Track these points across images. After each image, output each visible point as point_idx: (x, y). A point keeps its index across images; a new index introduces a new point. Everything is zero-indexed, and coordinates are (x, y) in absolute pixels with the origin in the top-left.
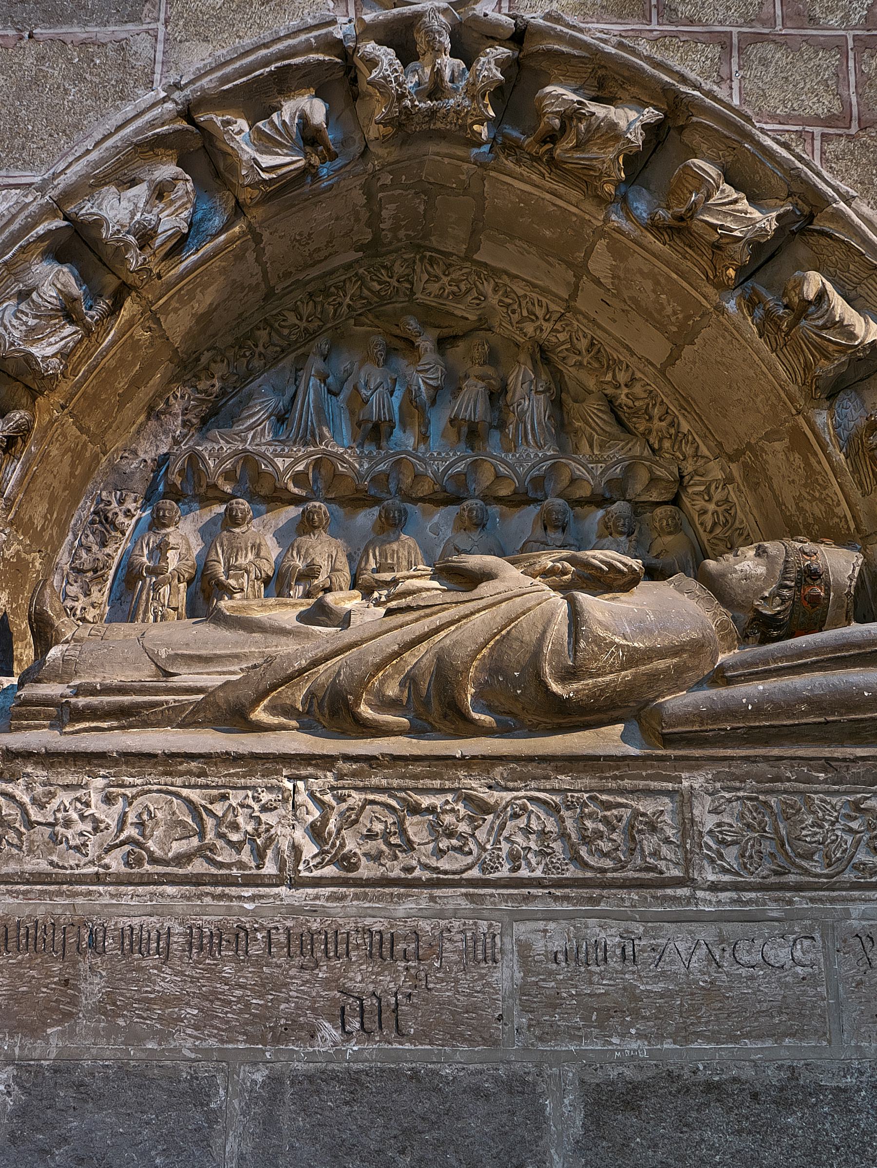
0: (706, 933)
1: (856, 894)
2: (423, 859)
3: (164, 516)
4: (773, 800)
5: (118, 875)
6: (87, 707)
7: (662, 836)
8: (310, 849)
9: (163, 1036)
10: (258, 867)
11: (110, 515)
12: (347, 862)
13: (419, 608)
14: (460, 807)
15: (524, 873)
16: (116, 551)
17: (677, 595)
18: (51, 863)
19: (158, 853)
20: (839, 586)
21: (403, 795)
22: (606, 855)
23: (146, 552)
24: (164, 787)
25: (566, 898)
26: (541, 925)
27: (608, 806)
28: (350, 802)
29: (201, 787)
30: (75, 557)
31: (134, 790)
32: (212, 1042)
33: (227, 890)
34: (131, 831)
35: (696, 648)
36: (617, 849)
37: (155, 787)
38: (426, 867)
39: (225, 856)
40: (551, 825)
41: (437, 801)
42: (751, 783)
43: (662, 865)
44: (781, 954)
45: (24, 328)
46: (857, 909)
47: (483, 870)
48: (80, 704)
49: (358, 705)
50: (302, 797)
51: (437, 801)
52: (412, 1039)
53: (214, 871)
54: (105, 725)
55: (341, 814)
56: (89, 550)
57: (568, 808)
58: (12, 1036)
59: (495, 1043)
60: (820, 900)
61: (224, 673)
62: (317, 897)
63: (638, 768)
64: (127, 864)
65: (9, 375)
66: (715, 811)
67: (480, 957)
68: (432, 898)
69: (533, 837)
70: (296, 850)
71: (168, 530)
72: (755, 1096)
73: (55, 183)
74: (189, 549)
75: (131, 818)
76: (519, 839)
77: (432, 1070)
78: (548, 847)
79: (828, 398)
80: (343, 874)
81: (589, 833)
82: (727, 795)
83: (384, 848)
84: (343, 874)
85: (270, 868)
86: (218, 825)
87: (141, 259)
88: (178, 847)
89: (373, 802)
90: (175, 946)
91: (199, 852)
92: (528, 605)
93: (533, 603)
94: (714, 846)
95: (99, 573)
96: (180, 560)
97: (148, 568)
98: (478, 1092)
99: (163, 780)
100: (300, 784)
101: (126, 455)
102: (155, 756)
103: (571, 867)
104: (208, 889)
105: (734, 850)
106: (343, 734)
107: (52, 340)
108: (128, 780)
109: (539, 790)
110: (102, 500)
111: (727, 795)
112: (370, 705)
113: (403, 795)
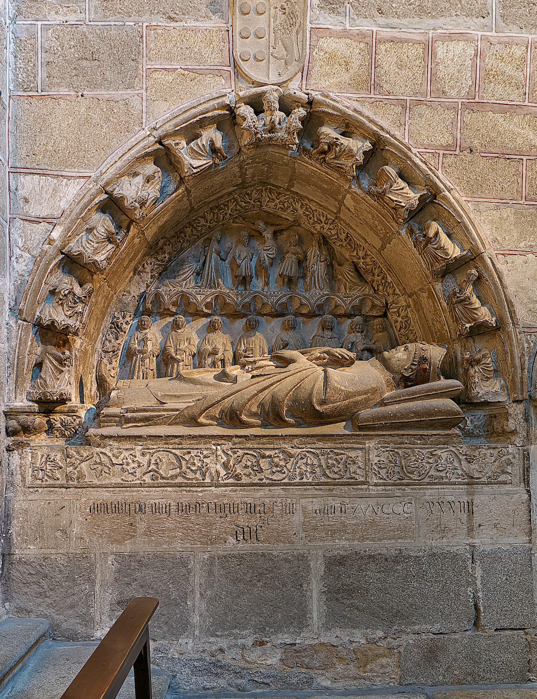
0: (372, 502)
1: (429, 486)
2: (266, 476)
3: (145, 324)
4: (400, 451)
5: (149, 484)
6: (132, 417)
7: (358, 466)
8: (223, 472)
9: (169, 543)
10: (203, 480)
11: (119, 324)
12: (237, 477)
13: (265, 375)
14: (281, 455)
15: (305, 480)
16: (122, 341)
17: (370, 368)
18: (122, 480)
19: (164, 475)
20: (435, 364)
21: (259, 451)
22: (336, 473)
23: (137, 342)
24: (165, 449)
25: (321, 489)
26: (311, 500)
27: (337, 454)
28: (238, 454)
29: (180, 449)
30: (104, 344)
31: (153, 451)
32: (188, 545)
33: (191, 489)
34: (153, 467)
35: (374, 391)
36: (340, 471)
37: (162, 449)
38: (268, 478)
39: (190, 475)
40: (315, 462)
41: (272, 453)
42: (392, 445)
43: (357, 476)
45: (92, 248)
46: (428, 492)
47: (289, 480)
48: (129, 416)
49: (241, 416)
50: (220, 452)
51: (272, 453)
52: (262, 542)
53: (186, 481)
54: (139, 425)
55: (234, 459)
56: (110, 342)
57: (322, 455)
58: (112, 544)
59: (293, 543)
61: (186, 402)
62: (226, 491)
63: (349, 439)
64: (152, 479)
65: (81, 265)
66: (378, 456)
67: (288, 512)
68: (270, 490)
69: (309, 466)
70: (217, 472)
71: (147, 331)
72: (386, 559)
73: (102, 177)
74: (157, 340)
75: (153, 461)
76: (303, 467)
77: (270, 553)
78: (314, 470)
79: (442, 277)
80: (236, 482)
81: (329, 465)
82: (383, 450)
83: (252, 472)
84: (236, 482)
85: (208, 480)
86: (187, 464)
87: (141, 213)
88: (171, 473)
89: (247, 454)
90: (172, 510)
91: (180, 474)
92: (308, 374)
93: (310, 373)
94: (377, 469)
95: (116, 353)
96: (153, 346)
97: (138, 350)
98: (286, 560)
99: (164, 446)
100: (219, 447)
101: (125, 293)
102: (162, 437)
103: (323, 478)
104: (184, 488)
105: (385, 470)
106: (235, 427)
107: (103, 252)
108: (151, 447)
109: (311, 448)
110: (115, 317)
111: (383, 450)
112: (246, 415)
113: (259, 451)
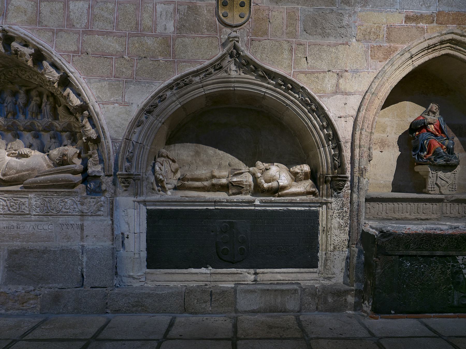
22: (15, 209)
27: (15, 200)
40: (5, 204)
42: (42, 196)
44: (46, 227)
46: (60, 219)
60: (54, 218)
105: (39, 208)
